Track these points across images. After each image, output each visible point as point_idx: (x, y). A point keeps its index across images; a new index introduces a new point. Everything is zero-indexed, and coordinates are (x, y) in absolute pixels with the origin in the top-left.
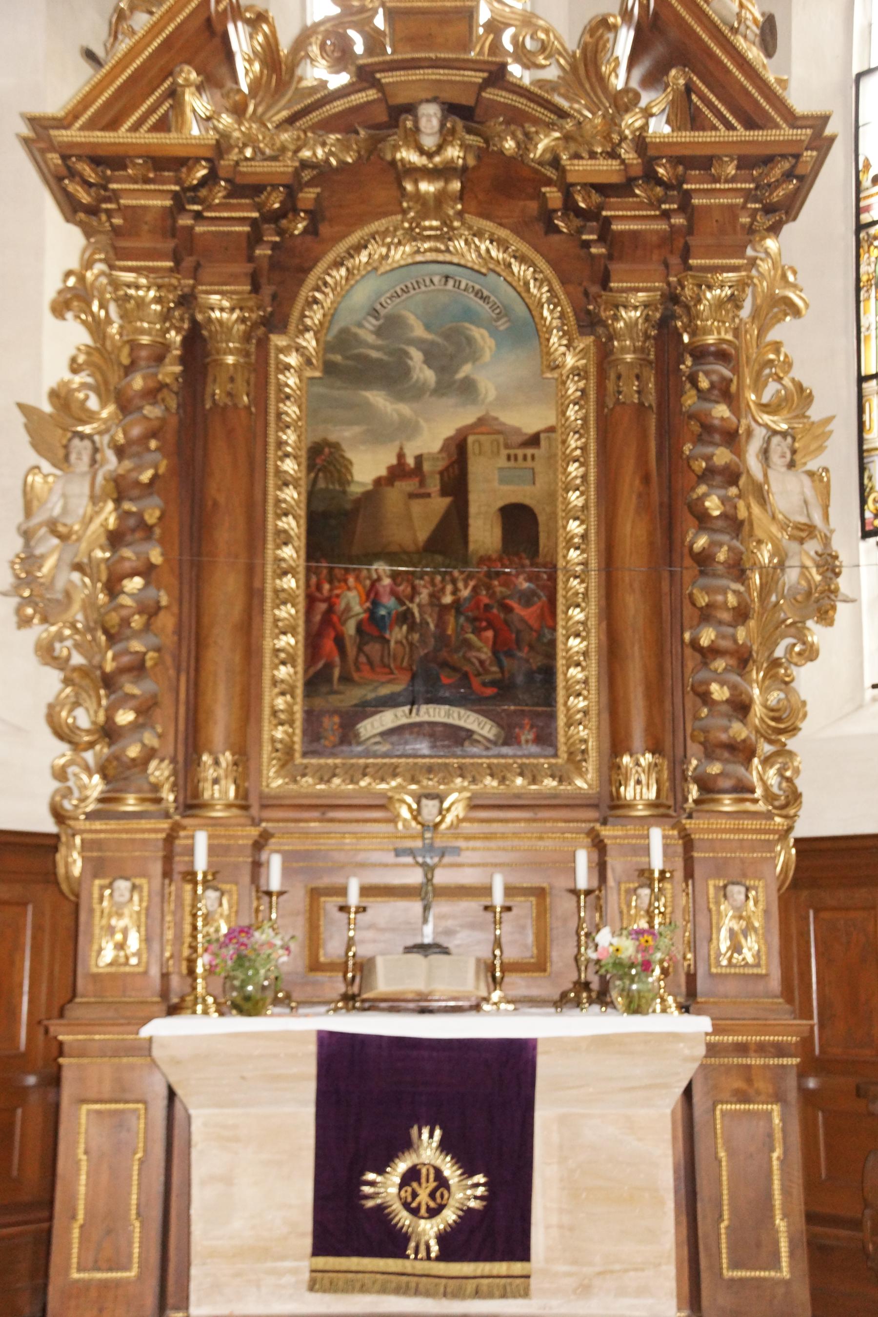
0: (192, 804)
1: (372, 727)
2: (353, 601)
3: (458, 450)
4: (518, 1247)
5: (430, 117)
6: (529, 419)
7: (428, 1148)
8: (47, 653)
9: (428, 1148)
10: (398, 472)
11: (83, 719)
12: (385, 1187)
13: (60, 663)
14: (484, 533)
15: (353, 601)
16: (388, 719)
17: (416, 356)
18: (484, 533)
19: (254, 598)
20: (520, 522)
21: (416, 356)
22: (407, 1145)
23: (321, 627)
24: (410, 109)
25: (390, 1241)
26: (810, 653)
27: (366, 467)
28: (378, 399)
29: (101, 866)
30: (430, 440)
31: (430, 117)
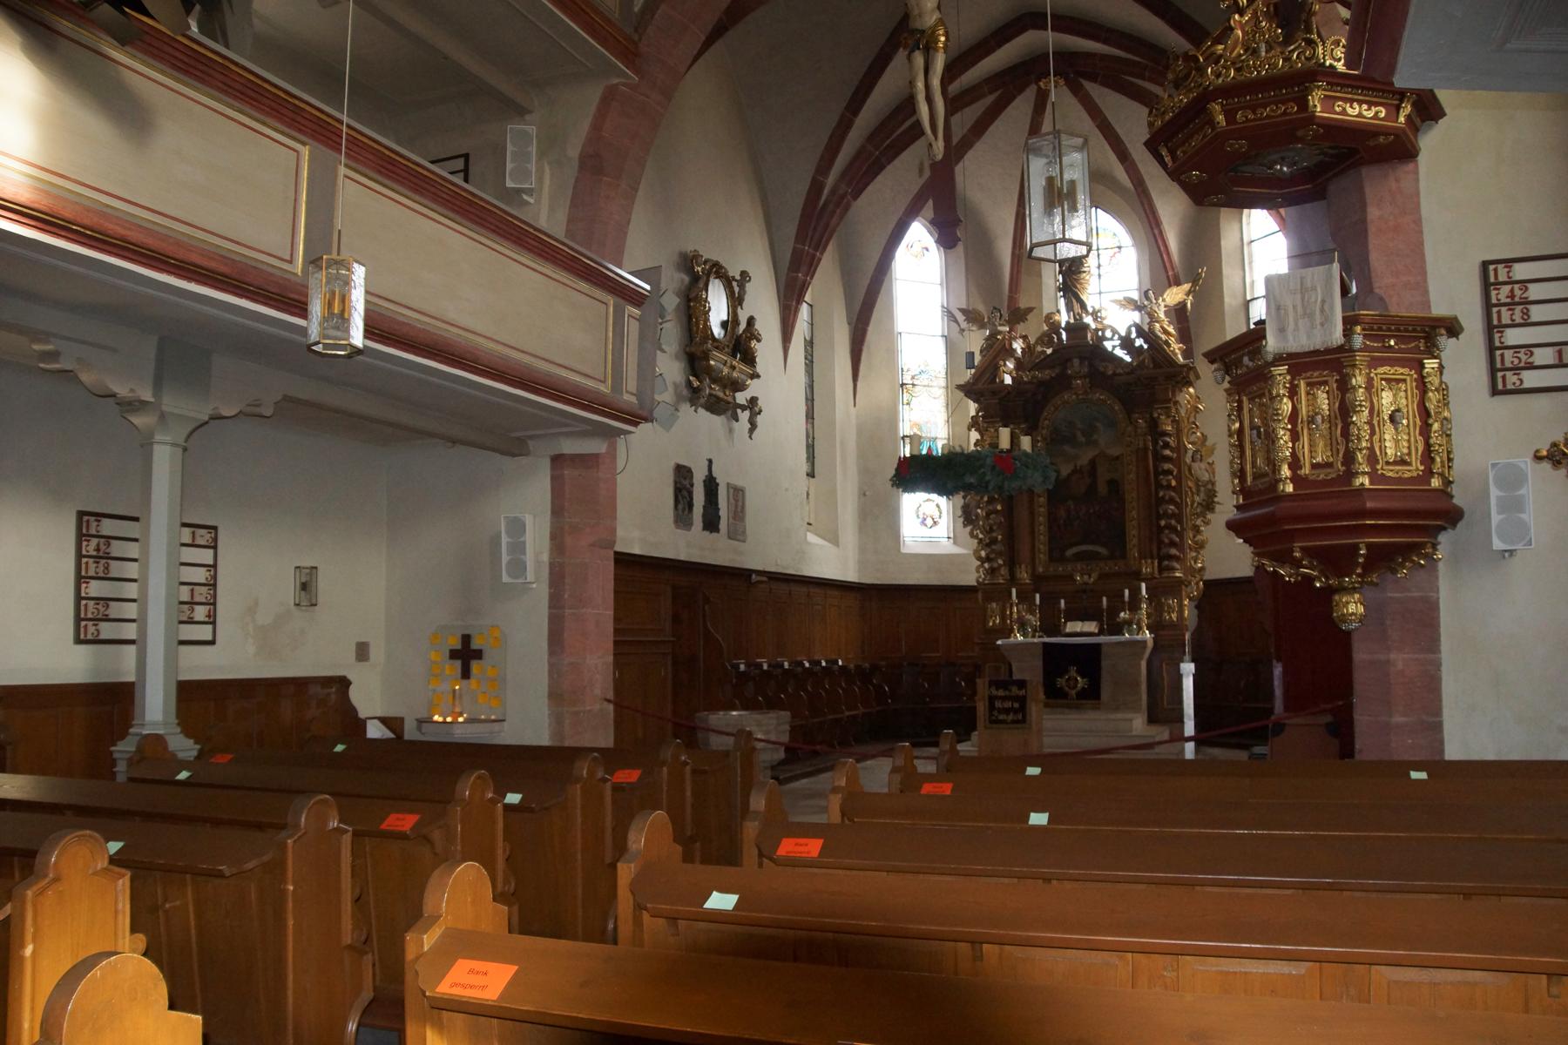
0: (1013, 580)
1: (1070, 552)
2: (1062, 513)
3: (1093, 463)
4: (1098, 697)
5: (1076, 362)
6: (1114, 451)
7: (1073, 671)
8: (972, 535)
9: (1073, 671)
10: (1075, 471)
11: (983, 554)
12: (1061, 682)
13: (976, 537)
14: (1103, 489)
15: (1062, 513)
16: (1074, 550)
17: (1079, 434)
18: (1103, 489)
19: (1032, 513)
20: (1115, 486)
21: (1079, 434)
22: (1067, 671)
23: (1052, 520)
24: (1069, 360)
25: (1065, 696)
26: (1207, 523)
27: (1065, 470)
28: (1067, 448)
29: (989, 598)
30: (1084, 460)
31: (1076, 362)
